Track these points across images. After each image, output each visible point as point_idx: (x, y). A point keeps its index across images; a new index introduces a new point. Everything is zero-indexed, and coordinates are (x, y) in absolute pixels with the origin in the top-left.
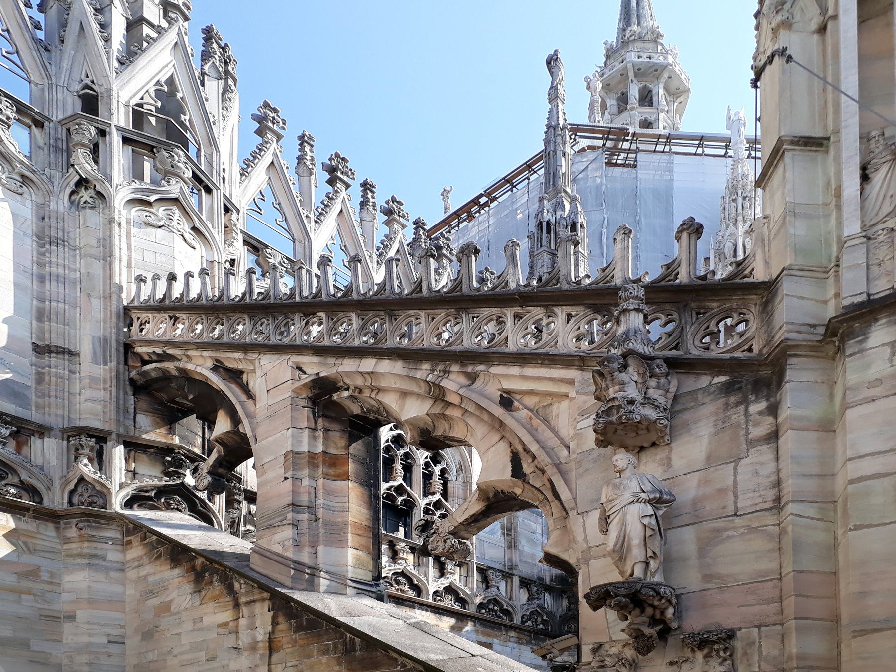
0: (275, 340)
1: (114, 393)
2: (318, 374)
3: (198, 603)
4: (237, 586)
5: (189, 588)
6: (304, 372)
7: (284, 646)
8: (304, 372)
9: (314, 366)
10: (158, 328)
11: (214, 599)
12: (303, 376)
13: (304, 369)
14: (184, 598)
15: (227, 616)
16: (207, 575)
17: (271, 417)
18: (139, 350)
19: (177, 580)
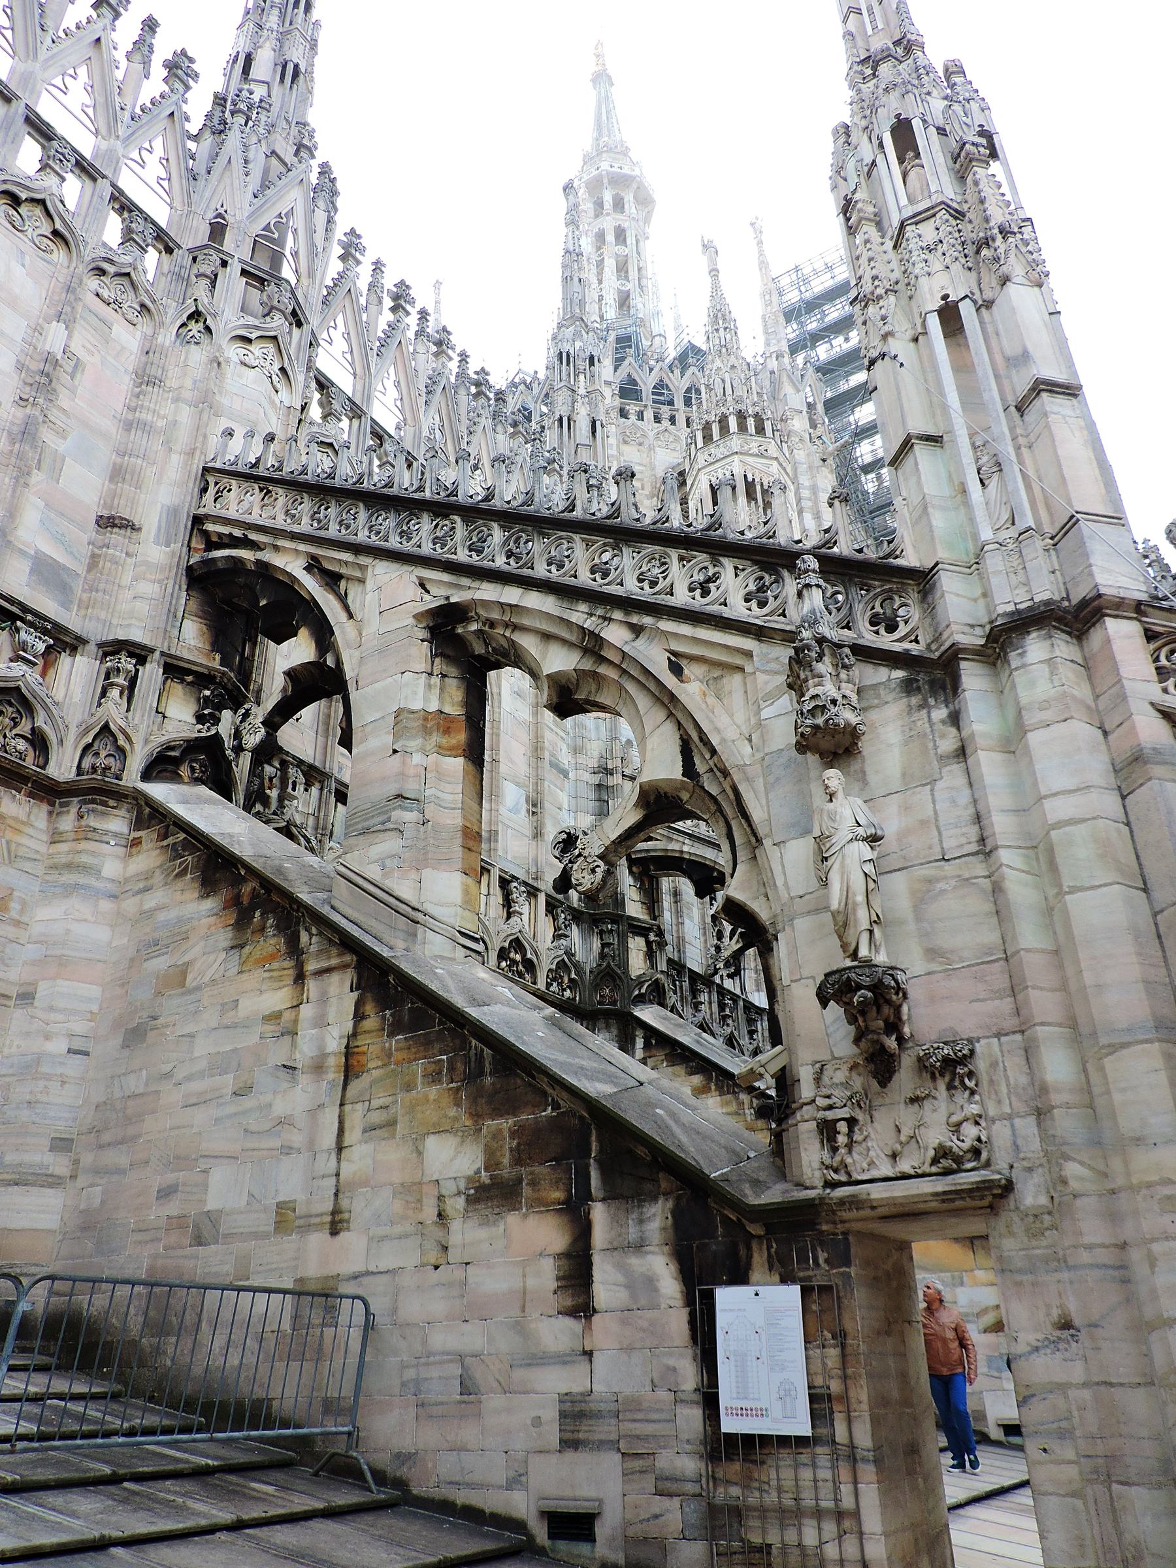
0: (394, 543)
1: (169, 590)
2: (448, 598)
3: (235, 970)
4: (304, 937)
5: (225, 937)
6: (428, 592)
7: (371, 1065)
8: (428, 592)
9: (447, 589)
10: (242, 504)
11: (262, 962)
12: (427, 597)
13: (428, 587)
14: (212, 957)
15: (278, 998)
16: (257, 914)
17: (383, 651)
18: (210, 527)
19: (205, 921)
